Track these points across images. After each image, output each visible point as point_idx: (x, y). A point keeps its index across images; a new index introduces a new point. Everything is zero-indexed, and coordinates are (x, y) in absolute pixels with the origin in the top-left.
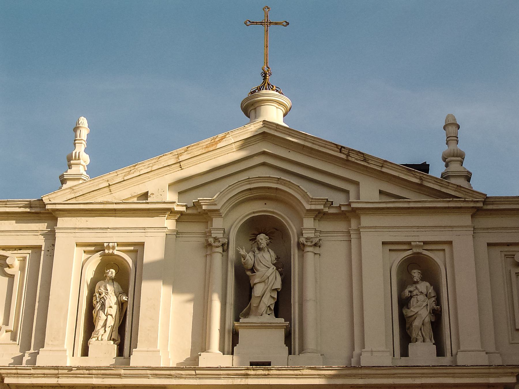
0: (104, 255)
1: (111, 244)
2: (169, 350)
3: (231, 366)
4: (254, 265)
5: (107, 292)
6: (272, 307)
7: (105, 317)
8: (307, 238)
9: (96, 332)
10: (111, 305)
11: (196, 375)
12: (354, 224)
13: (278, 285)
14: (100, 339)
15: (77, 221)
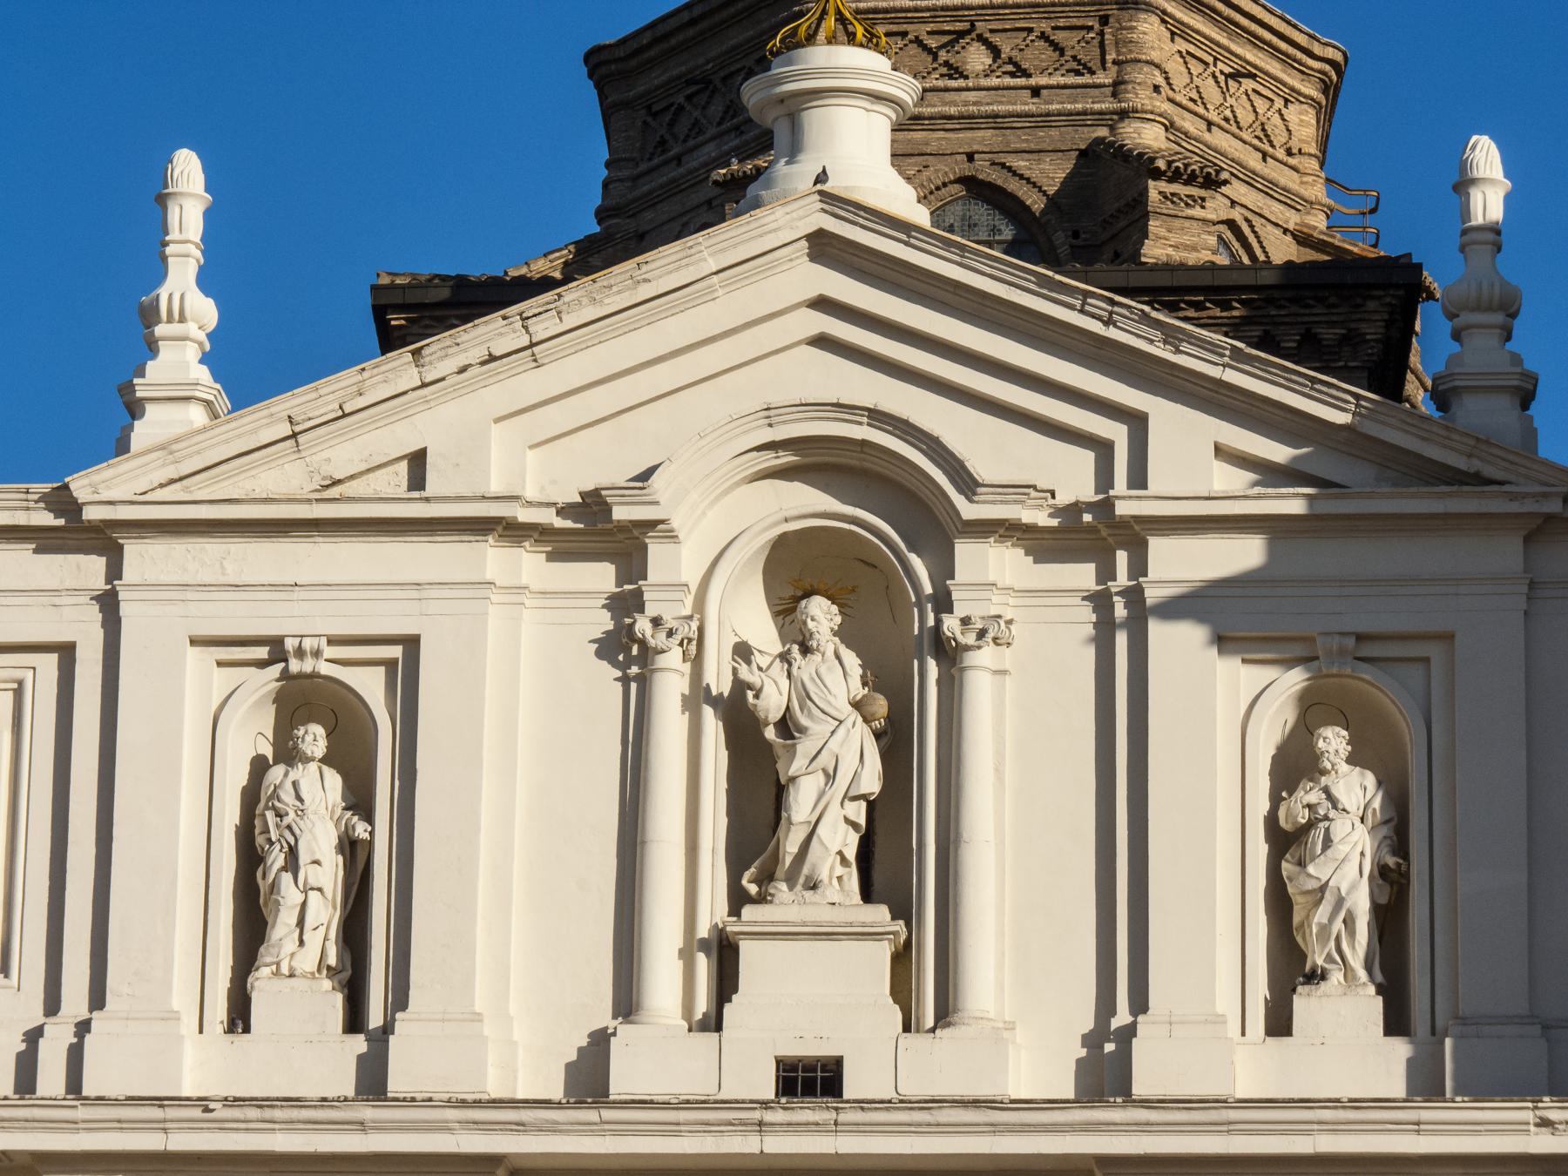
0: (285, 675)
1: (308, 644)
2: (513, 1009)
3: (712, 1089)
4: (788, 708)
5: (301, 808)
6: (851, 854)
7: (300, 898)
8: (965, 621)
9: (273, 946)
10: (318, 856)
11: (603, 1122)
12: (1122, 557)
13: (872, 783)
14: (285, 970)
15: (189, 557)
